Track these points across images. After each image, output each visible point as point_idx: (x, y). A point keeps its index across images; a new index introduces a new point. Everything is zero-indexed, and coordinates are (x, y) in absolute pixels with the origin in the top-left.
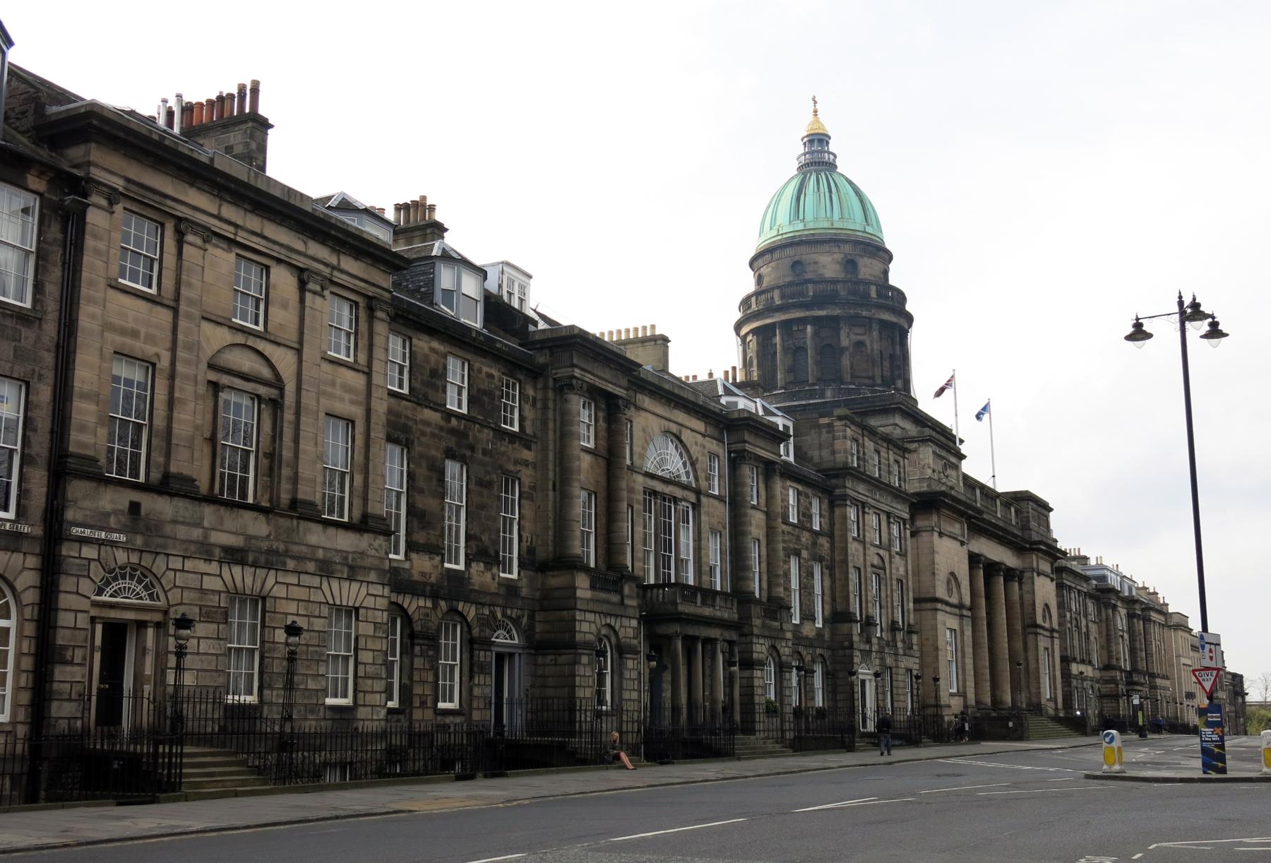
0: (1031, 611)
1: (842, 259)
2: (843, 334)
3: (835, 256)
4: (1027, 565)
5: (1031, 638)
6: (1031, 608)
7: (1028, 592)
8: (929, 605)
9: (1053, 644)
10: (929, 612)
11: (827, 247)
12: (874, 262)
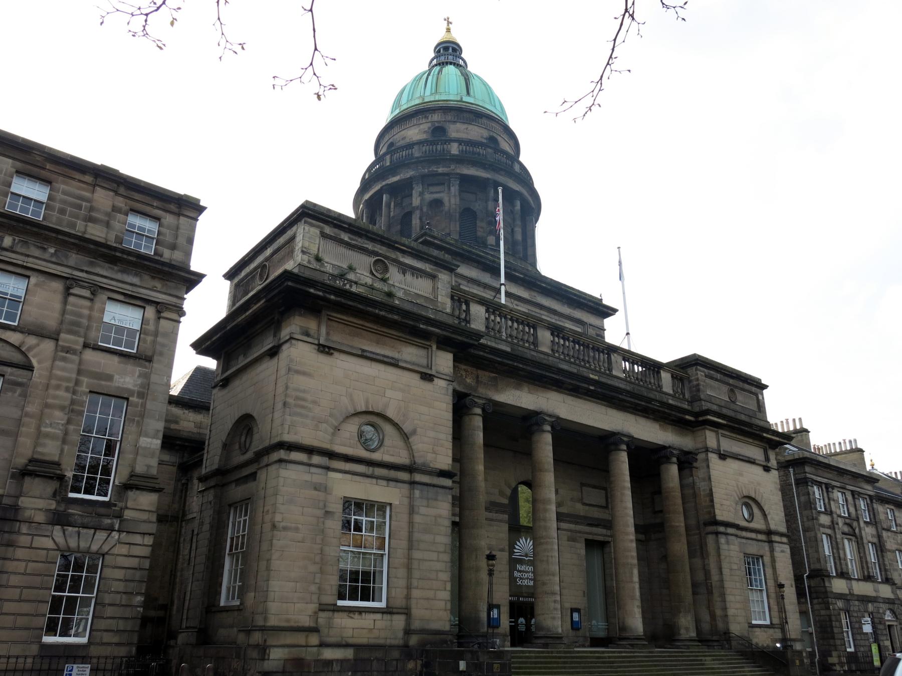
1: (429, 128)
2: (415, 193)
3: (422, 127)
4: (700, 445)
5: (710, 539)
6: (708, 499)
8: (275, 456)
9: (772, 550)
11: (414, 121)
12: (470, 127)
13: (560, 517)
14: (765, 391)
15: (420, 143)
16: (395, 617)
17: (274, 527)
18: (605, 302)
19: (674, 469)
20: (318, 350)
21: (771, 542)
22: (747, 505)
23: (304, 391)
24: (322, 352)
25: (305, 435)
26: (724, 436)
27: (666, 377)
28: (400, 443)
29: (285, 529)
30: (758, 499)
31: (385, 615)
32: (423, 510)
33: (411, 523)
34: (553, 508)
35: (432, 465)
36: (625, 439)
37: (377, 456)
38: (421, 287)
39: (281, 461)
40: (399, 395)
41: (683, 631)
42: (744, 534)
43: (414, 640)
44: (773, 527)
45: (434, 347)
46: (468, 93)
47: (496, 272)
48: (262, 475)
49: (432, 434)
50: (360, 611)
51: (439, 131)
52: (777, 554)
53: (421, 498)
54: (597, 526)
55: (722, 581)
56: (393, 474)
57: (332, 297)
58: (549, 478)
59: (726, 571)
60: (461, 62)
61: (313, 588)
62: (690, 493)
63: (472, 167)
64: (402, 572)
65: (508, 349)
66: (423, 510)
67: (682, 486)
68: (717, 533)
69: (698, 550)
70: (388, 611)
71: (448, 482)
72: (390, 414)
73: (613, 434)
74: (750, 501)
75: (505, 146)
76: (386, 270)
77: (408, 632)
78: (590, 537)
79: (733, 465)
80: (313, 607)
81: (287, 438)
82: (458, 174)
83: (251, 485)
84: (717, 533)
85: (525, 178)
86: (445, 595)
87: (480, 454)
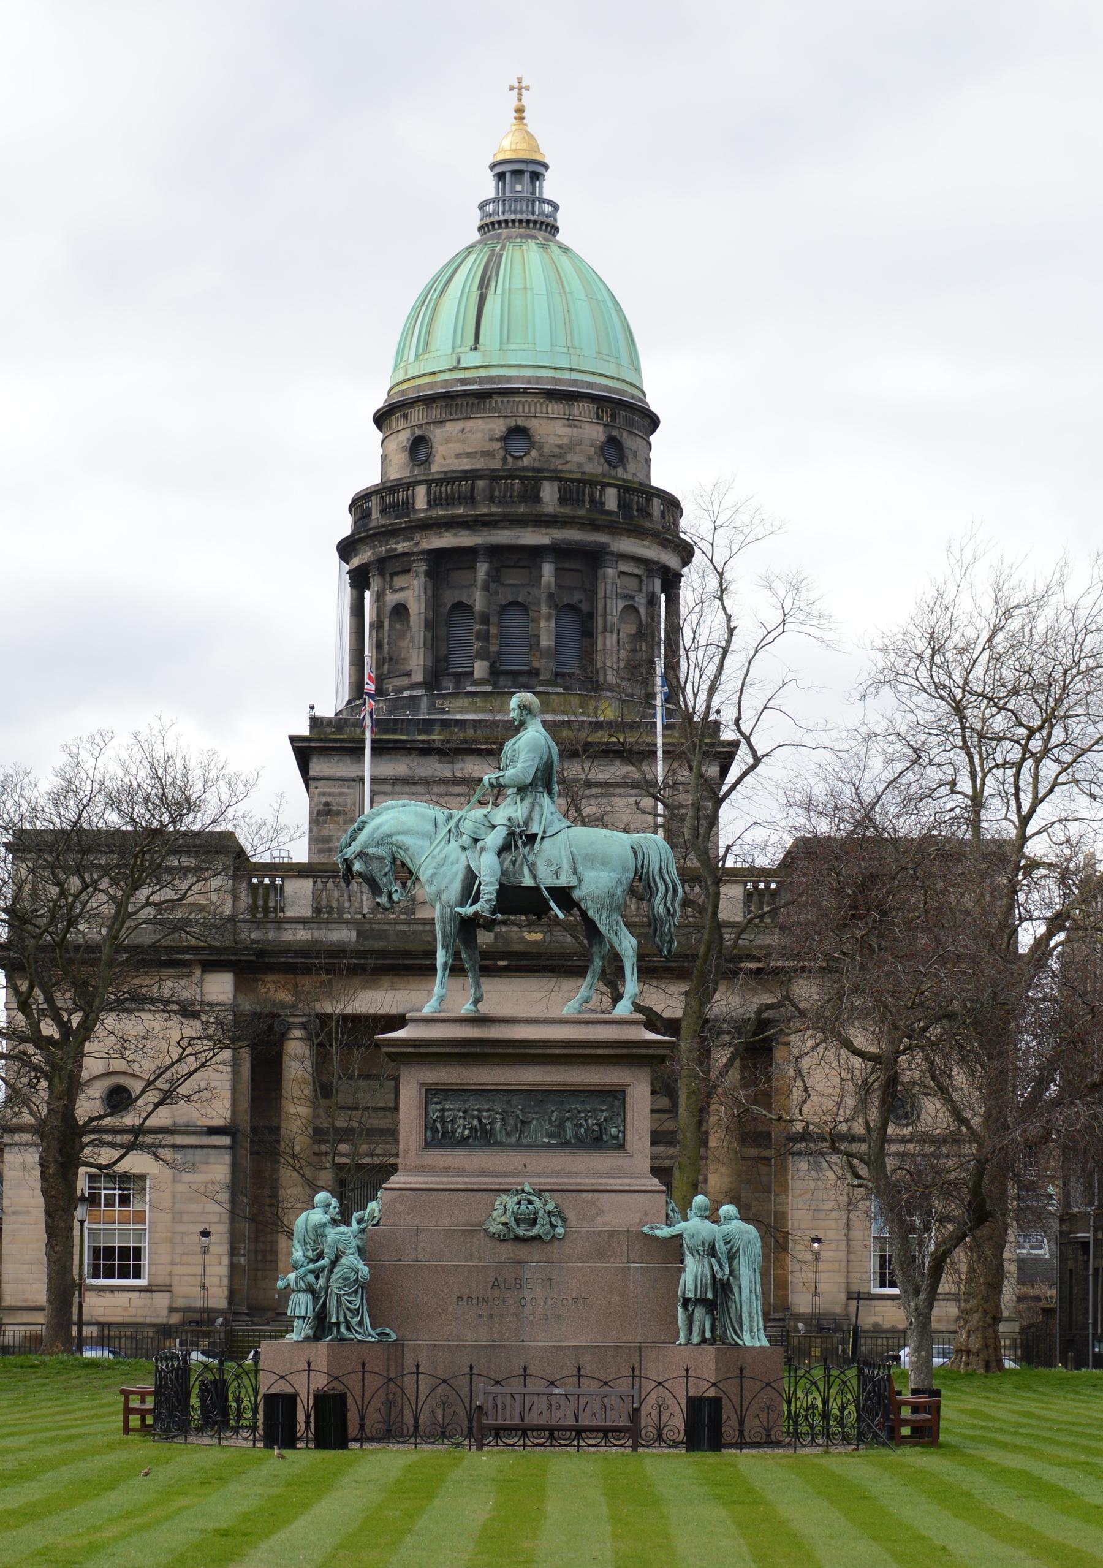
12: (469, 424)
29: (14, 1213)
31: (143, 1294)
35: (199, 1123)
50: (112, 1289)
63: (446, 531)
71: (226, 1140)
77: (172, 1310)
82: (422, 552)
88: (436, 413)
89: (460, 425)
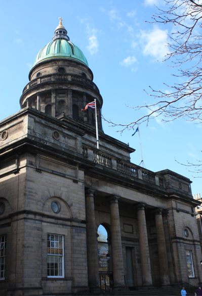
0: (173, 230)
4: (169, 207)
5: (174, 245)
7: (171, 221)
8: (22, 216)
9: (195, 248)
10: (21, 221)
12: (75, 69)
13: (123, 238)
14: (191, 184)
15: (54, 75)
16: (68, 281)
17: (24, 246)
18: (130, 146)
19: (161, 217)
20: (36, 171)
21: (194, 245)
22: (186, 230)
23: (32, 189)
24: (38, 172)
25: (34, 207)
26: (178, 202)
27: (157, 178)
28: (66, 209)
29: (28, 247)
30: (190, 227)
32: (76, 237)
33: (72, 243)
34: (120, 234)
36: (144, 205)
37: (58, 215)
38: (71, 143)
39: (25, 218)
40: (65, 189)
41: (165, 282)
42: (185, 242)
43: (76, 291)
44: (195, 239)
45: (78, 169)
46: (73, 53)
47: (96, 137)
48: (14, 224)
49: (78, 205)
51: (61, 70)
52: (197, 249)
53: (76, 232)
54: (130, 241)
55: (179, 261)
56: (65, 222)
57: (42, 149)
58: (118, 222)
59: (180, 257)
60: (66, 37)
61: (39, 271)
62: (166, 225)
64: (70, 263)
65: (102, 169)
66: (76, 237)
67: (164, 223)
68: (177, 242)
69: (170, 249)
70: (66, 279)
71: (84, 225)
72: (63, 197)
73: (139, 203)
74: (187, 229)
75: (89, 77)
76: (58, 136)
77: (73, 287)
78: (127, 246)
79: (181, 214)
80: (40, 279)
81: (27, 209)
82: (71, 90)
83: (8, 229)
84: (177, 242)
85: (97, 91)
86: (86, 272)
87: (93, 212)
88: (66, 63)
89: (73, 68)
